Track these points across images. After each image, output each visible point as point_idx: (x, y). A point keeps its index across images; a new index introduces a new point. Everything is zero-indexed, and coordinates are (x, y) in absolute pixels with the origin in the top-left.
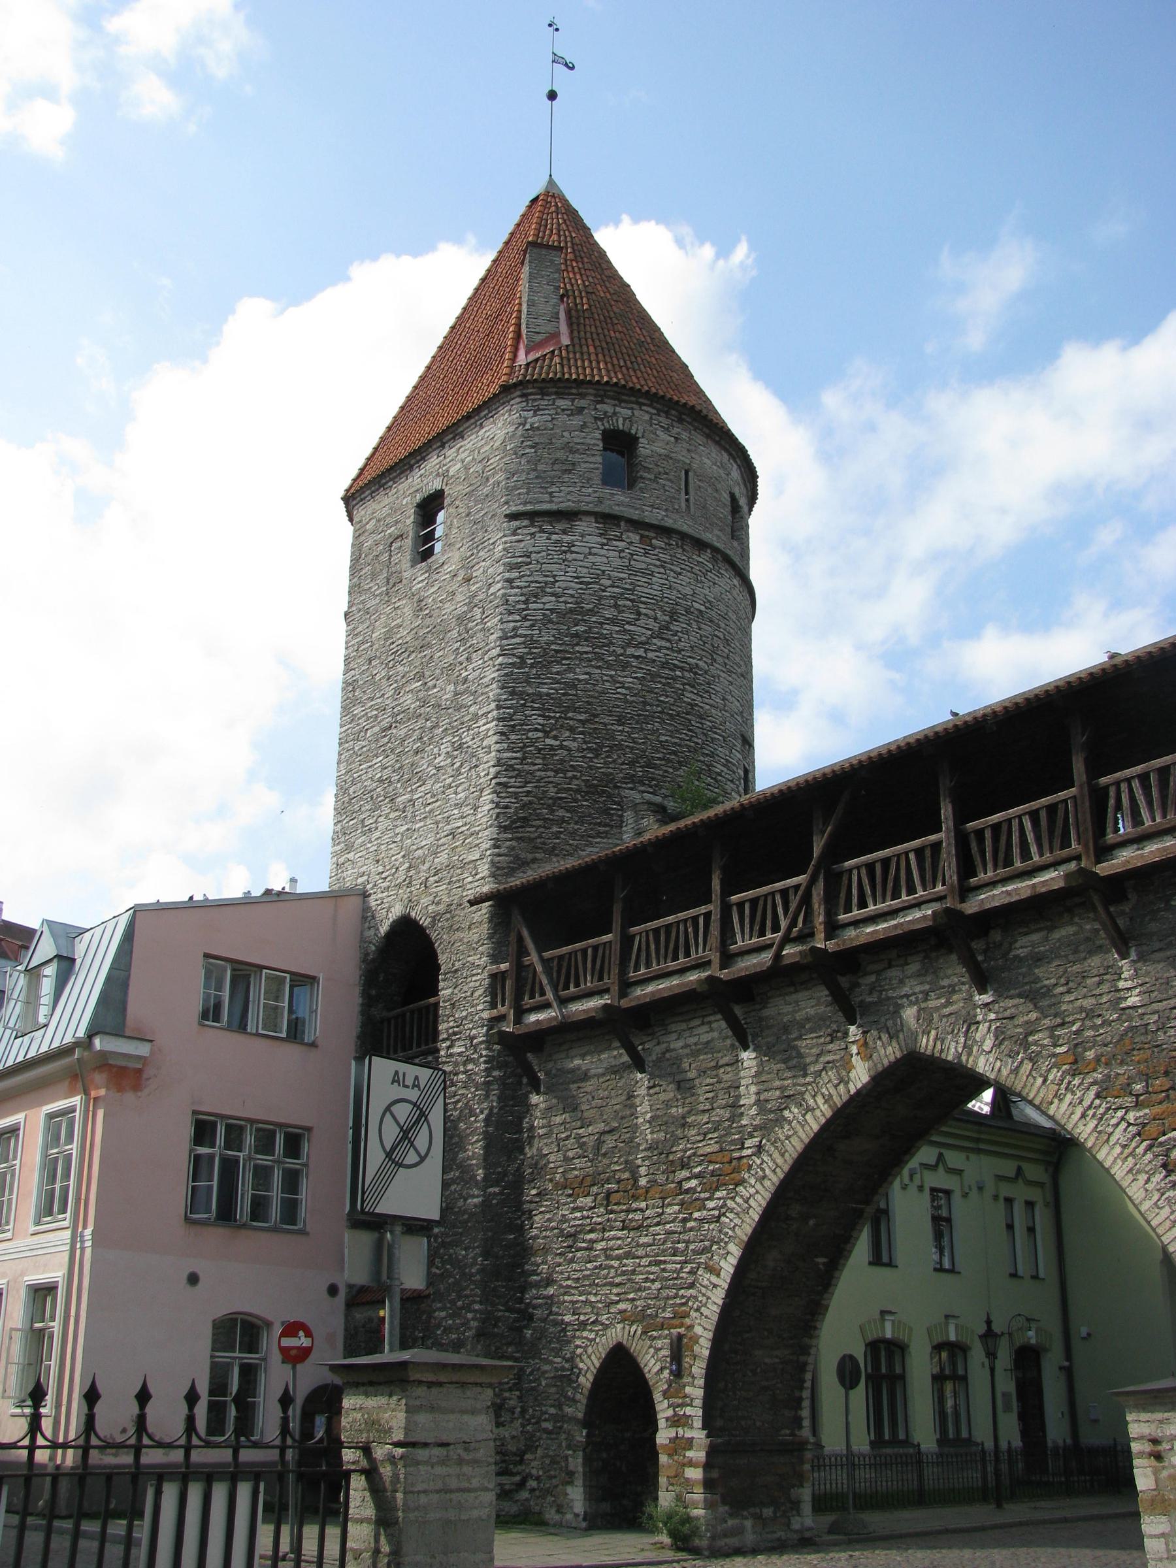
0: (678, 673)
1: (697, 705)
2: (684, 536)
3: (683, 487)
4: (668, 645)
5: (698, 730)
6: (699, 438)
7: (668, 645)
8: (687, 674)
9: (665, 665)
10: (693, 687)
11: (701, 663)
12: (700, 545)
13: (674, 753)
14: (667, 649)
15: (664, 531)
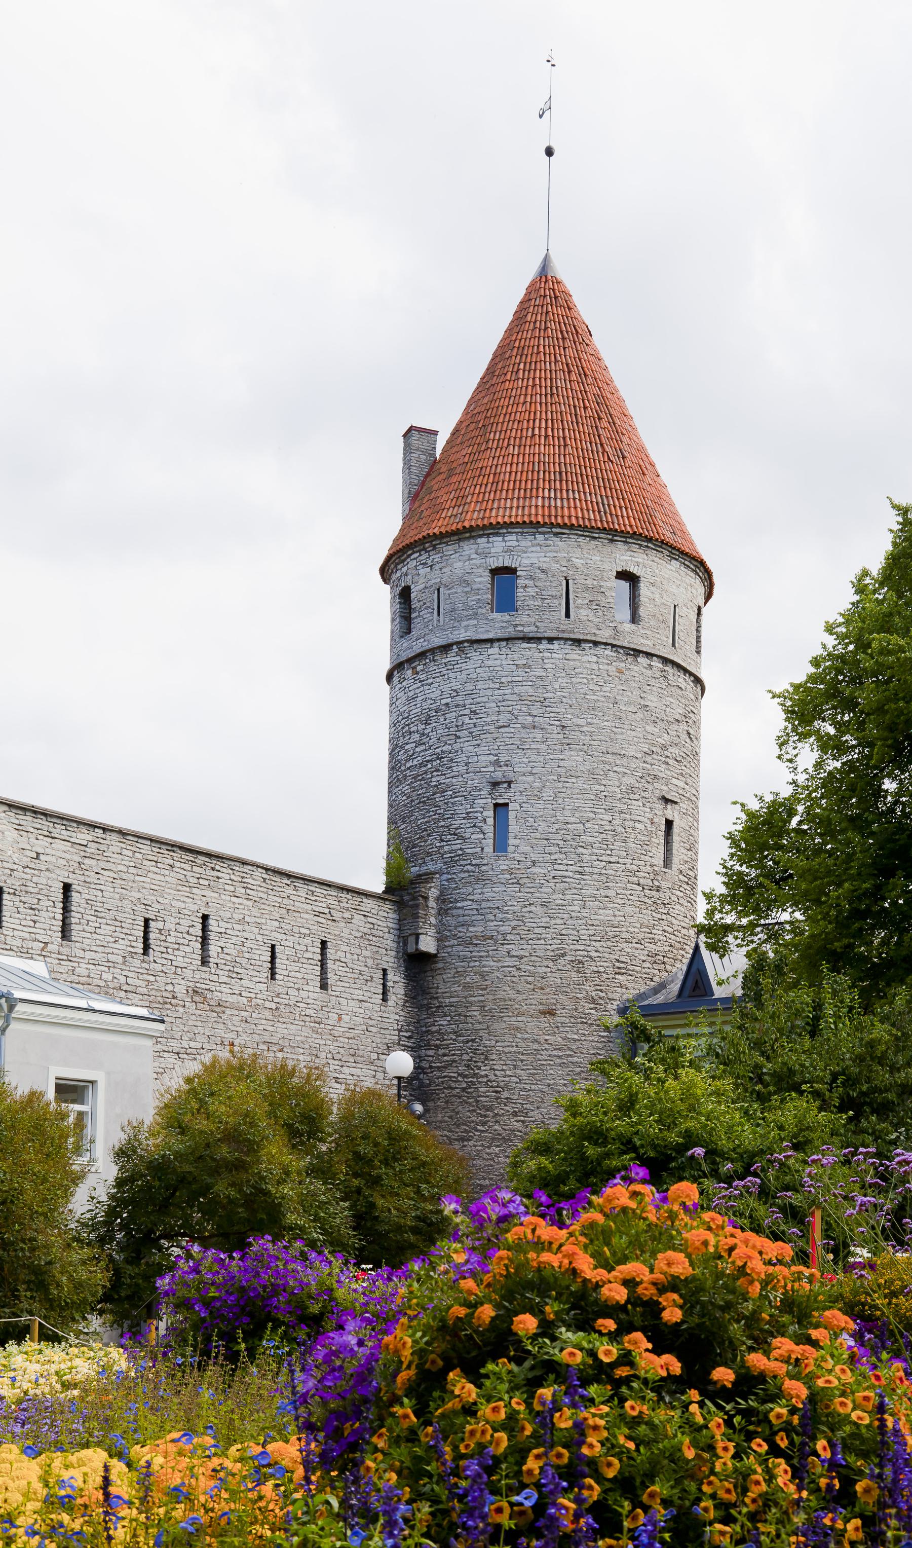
0: (429, 766)
1: (440, 784)
2: (432, 651)
3: (436, 607)
4: (423, 748)
5: (441, 803)
6: (449, 550)
7: (423, 748)
8: (435, 763)
9: (421, 765)
10: (438, 770)
11: (445, 748)
12: (446, 648)
13: (426, 830)
14: (423, 751)
15: (422, 655)
